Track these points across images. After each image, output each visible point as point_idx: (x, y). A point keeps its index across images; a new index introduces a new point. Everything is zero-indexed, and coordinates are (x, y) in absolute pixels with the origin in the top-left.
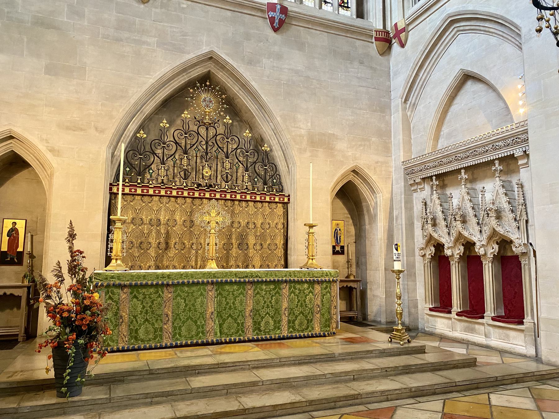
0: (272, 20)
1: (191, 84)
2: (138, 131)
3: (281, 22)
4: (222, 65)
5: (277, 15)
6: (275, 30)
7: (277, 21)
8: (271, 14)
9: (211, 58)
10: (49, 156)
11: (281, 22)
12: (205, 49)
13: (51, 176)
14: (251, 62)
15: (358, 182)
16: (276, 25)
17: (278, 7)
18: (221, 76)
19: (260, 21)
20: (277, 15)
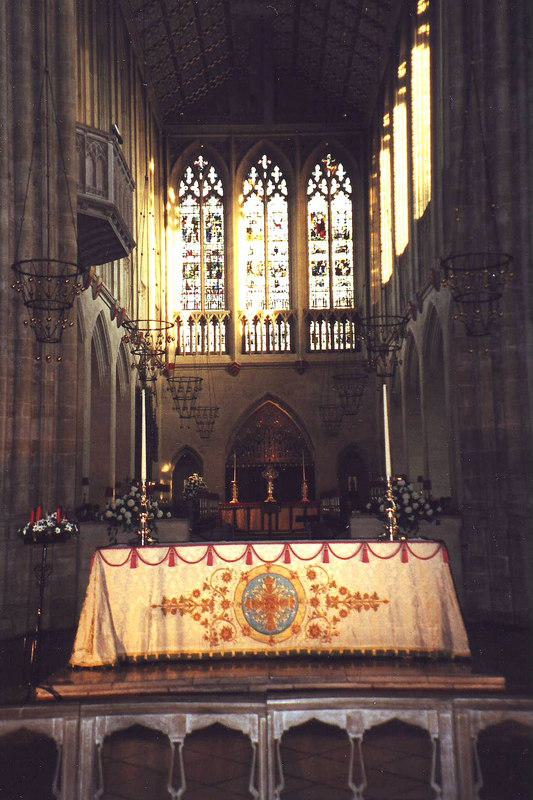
0: (299, 370)
6: (301, 374)
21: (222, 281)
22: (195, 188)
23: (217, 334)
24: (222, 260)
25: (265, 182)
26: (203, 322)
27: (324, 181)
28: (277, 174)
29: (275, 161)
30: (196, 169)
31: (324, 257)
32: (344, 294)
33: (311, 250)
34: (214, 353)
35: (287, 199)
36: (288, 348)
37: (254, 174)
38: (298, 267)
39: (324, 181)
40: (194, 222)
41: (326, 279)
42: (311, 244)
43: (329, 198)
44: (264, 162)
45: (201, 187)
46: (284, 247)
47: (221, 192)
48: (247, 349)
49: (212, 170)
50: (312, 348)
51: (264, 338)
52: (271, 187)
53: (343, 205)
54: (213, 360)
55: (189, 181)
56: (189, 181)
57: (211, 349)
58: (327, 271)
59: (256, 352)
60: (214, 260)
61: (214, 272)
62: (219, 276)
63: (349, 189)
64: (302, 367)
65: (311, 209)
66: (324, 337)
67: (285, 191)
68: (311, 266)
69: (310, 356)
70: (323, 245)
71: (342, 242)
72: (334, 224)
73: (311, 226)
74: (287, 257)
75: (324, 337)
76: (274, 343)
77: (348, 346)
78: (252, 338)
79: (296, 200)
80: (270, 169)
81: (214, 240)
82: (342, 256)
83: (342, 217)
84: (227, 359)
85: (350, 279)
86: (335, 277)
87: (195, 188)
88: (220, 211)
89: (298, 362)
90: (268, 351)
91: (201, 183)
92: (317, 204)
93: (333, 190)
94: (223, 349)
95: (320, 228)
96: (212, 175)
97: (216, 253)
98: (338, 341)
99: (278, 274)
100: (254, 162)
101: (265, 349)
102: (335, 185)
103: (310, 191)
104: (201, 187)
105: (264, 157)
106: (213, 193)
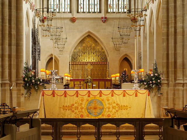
0: (103, 21)
1: (85, 38)
2: (74, 50)
3: (105, 21)
4: (92, 33)
5: (104, 20)
6: (104, 23)
7: (104, 21)
8: (102, 19)
9: (89, 32)
10: (58, 58)
11: (105, 21)
12: (87, 31)
13: (59, 62)
14: (98, 32)
15: (128, 57)
16: (104, 21)
17: (104, 18)
18: (91, 35)
19: (100, 21)
20: (104, 20)
23: (66, 4)
34: (64, 12)
36: (98, 11)
48: (79, 11)
50: (109, 11)
51: (87, 6)
54: (65, 16)
57: (63, 11)
59: (84, 12)
64: (105, 20)
66: (115, 6)
69: (108, 14)
75: (115, 6)
76: (92, 8)
77: (125, 10)
78: (82, 6)
84: (70, 16)
89: (102, 18)
90: (89, 12)
94: (69, 11)
98: (121, 8)
101: (87, 11)
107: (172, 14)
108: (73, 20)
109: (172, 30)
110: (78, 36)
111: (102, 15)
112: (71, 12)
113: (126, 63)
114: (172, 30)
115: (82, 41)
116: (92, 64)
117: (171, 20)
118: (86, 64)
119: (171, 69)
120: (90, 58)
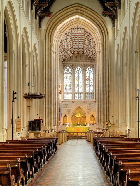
9: (79, 106)
21: (71, 87)
22: (67, 72)
24: (71, 84)
25: (79, 71)
26: (68, 94)
27: (89, 71)
28: (81, 69)
29: (80, 67)
30: (67, 69)
31: (88, 83)
32: (92, 90)
33: (86, 82)
35: (82, 74)
37: (77, 70)
38: (84, 85)
39: (89, 71)
40: (67, 77)
41: (89, 87)
42: (86, 81)
43: (89, 74)
44: (79, 68)
45: (68, 72)
46: (82, 82)
47: (71, 72)
49: (70, 69)
52: (80, 72)
53: (92, 75)
55: (66, 71)
56: (66, 71)
58: (89, 86)
60: (70, 84)
61: (70, 86)
62: (71, 86)
63: (93, 72)
64: (84, 102)
65: (86, 75)
67: (82, 72)
68: (86, 85)
70: (88, 81)
71: (91, 81)
72: (90, 78)
73: (86, 78)
74: (82, 83)
77: (92, 98)
79: (84, 74)
80: (80, 69)
81: (70, 80)
82: (91, 83)
83: (91, 77)
84: (72, 100)
85: (92, 87)
86: (90, 87)
87: (67, 72)
88: (71, 76)
91: (68, 71)
92: (87, 75)
93: (90, 72)
95: (88, 79)
96: (70, 70)
97: (70, 82)
99: (81, 86)
100: (77, 68)
102: (90, 72)
103: (86, 72)
104: (68, 72)
105: (79, 67)
106: (70, 72)
107: (99, 106)
108: (73, 102)
109: (99, 110)
110: (75, 108)
111: (84, 100)
112: (72, 99)
113: (92, 117)
114: (99, 110)
115: (76, 109)
116: (80, 117)
117: (99, 108)
118: (78, 117)
119: (99, 121)
120: (79, 116)
